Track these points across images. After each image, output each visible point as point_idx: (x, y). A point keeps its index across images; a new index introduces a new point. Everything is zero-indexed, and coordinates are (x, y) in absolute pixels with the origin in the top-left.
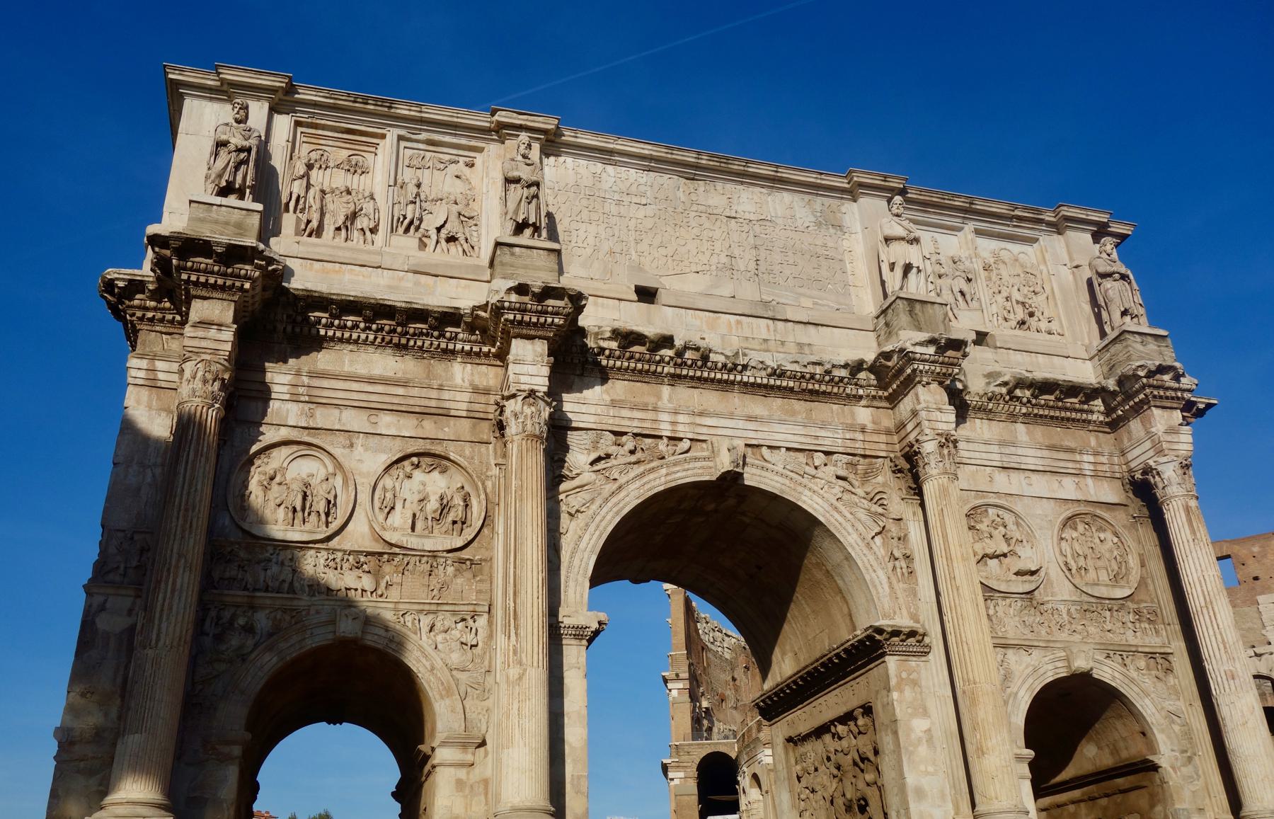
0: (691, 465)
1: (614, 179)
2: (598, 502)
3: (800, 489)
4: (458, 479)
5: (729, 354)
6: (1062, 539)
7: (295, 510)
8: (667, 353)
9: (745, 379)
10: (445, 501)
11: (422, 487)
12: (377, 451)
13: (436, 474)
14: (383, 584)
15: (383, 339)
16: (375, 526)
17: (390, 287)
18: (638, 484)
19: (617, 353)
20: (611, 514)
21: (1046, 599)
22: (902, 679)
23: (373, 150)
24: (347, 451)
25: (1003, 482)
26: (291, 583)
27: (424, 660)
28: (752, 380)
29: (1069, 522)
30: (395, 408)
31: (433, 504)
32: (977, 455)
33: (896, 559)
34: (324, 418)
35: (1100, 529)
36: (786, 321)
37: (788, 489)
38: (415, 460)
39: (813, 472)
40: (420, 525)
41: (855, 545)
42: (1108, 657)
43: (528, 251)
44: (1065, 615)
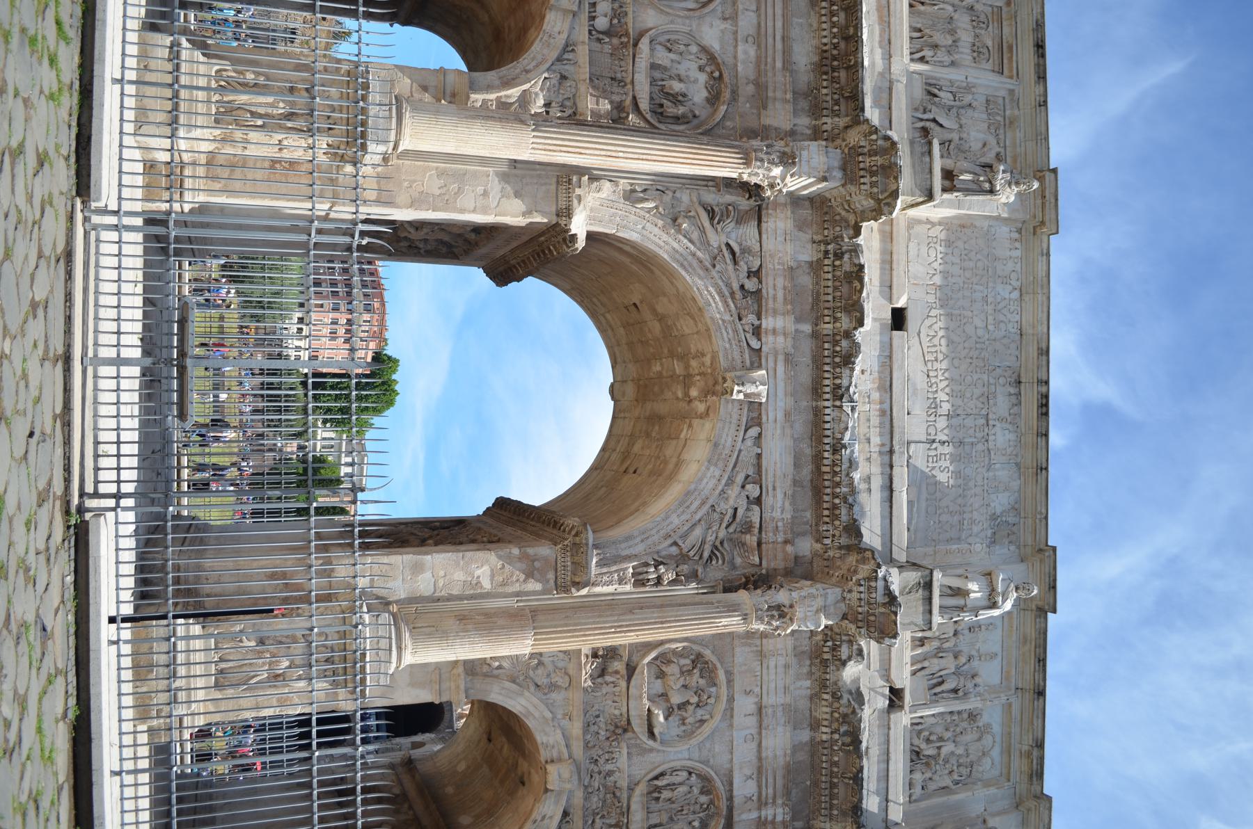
1: (1007, 296)
3: (721, 464)
5: (852, 390)
6: (690, 773)
9: (827, 411)
10: (680, 98)
11: (692, 79)
13: (705, 94)
15: (826, 51)
19: (838, 273)
20: (681, 259)
22: (533, 561)
23: (996, 69)
24: (719, 14)
25: (745, 705)
27: (534, 64)
31: (677, 86)
32: (772, 677)
37: (719, 451)
38: (717, 74)
40: (657, 75)
43: (927, 170)
44: (609, 767)
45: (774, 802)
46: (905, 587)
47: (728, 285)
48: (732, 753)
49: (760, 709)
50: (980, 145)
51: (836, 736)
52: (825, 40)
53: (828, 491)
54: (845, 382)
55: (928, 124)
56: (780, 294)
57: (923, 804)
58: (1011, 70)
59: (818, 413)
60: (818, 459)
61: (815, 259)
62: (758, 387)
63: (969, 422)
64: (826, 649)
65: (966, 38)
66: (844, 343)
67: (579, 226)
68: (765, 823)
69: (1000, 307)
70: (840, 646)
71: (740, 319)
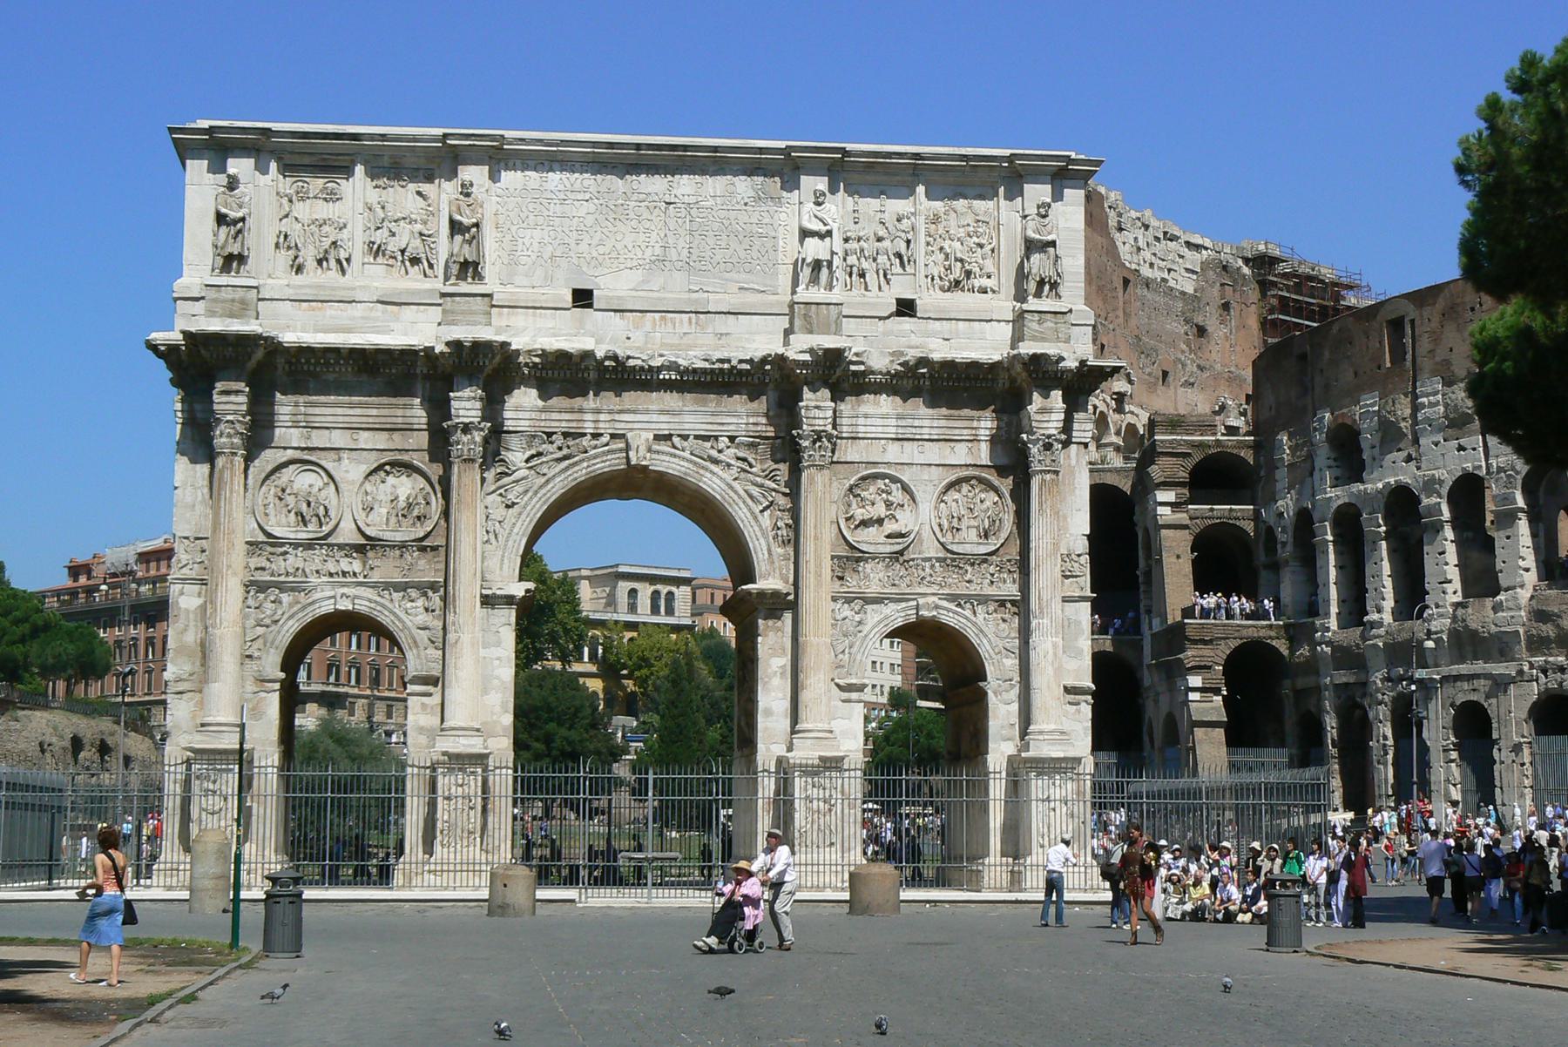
0: (609, 457)
2: (530, 494)
3: (702, 472)
4: (422, 482)
5: (645, 358)
6: (942, 501)
7: (303, 517)
12: (360, 462)
13: (404, 477)
14: (368, 567)
16: (359, 524)
17: (362, 318)
18: (563, 476)
19: (548, 367)
21: (912, 556)
25: (894, 453)
26: (303, 570)
28: (667, 377)
29: (953, 485)
30: (371, 426)
31: (402, 504)
32: (873, 429)
33: (778, 529)
34: (318, 439)
36: (709, 312)
38: (387, 468)
39: (714, 453)
42: (959, 605)
45: (976, 428)
47: (559, 460)
48: (930, 465)
50: (418, 198)
51: (927, 375)
52: (350, 369)
54: (639, 362)
57: (1003, 280)
58: (345, 160)
61: (535, 382)
62: (640, 439)
63: (672, 224)
64: (856, 381)
65: (323, 210)
66: (607, 363)
67: (519, 589)
69: (568, 185)
71: (586, 452)
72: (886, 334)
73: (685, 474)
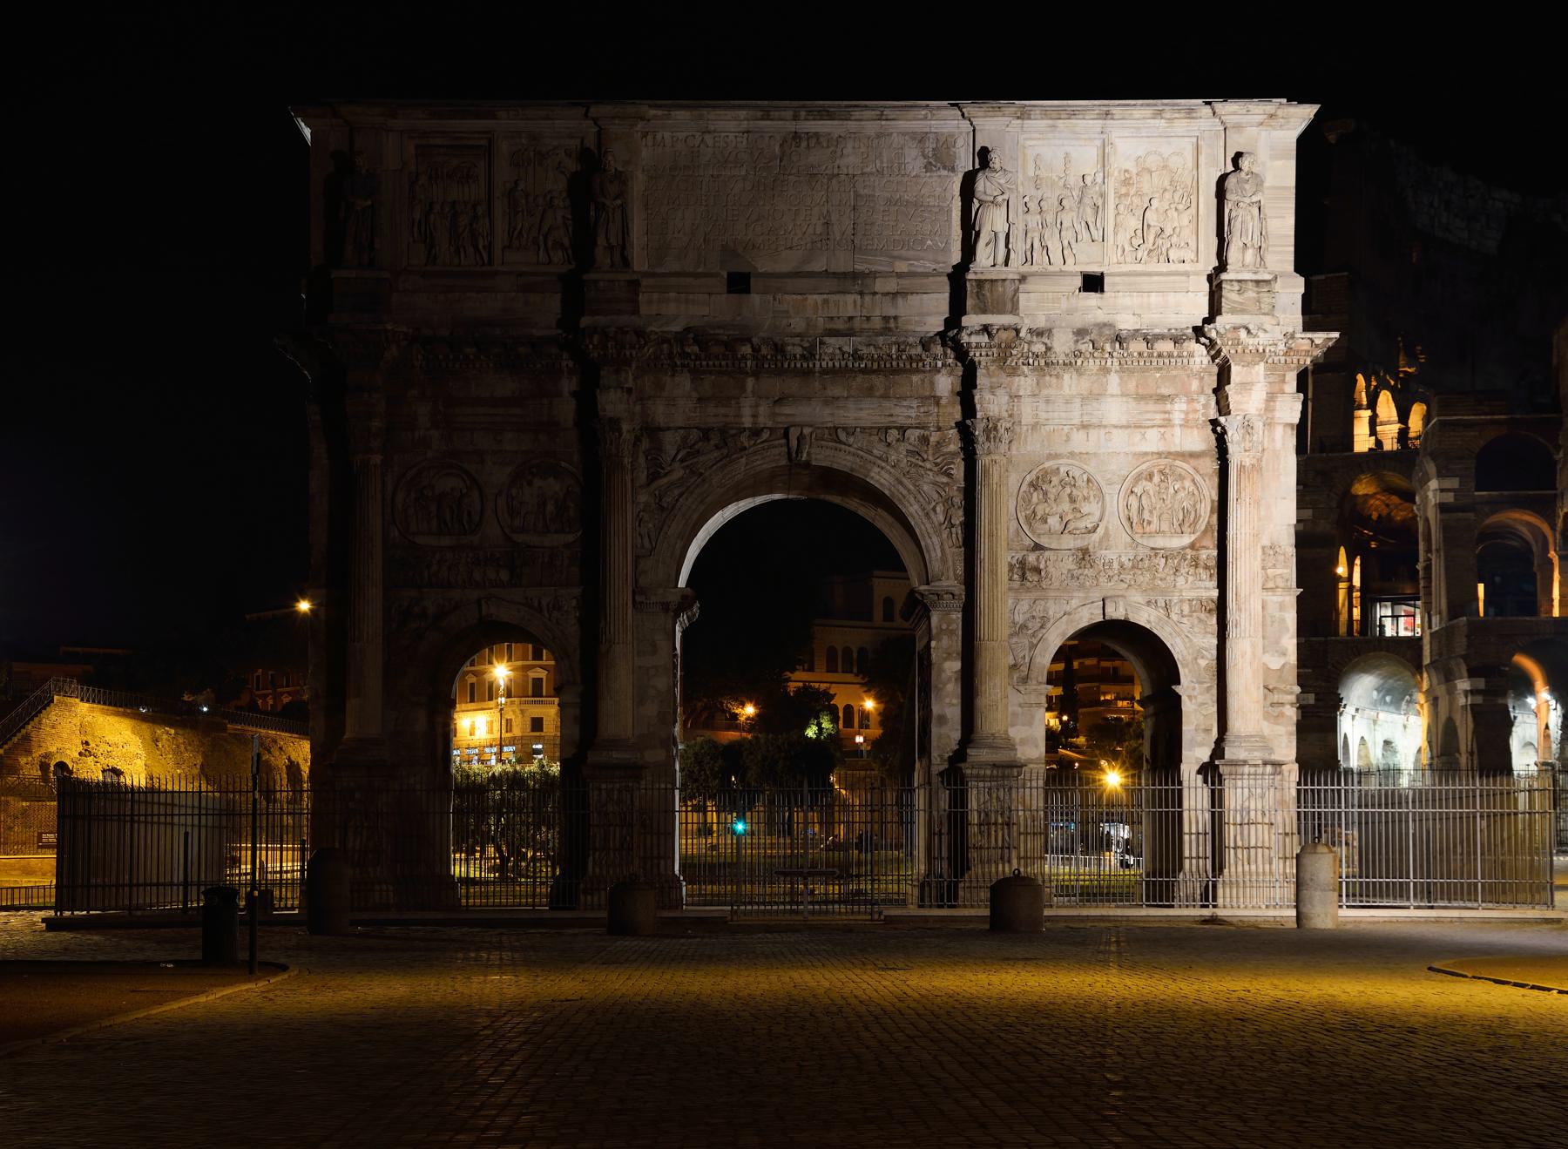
8: (746, 350)
13: (551, 480)
19: (703, 356)
31: (550, 507)
35: (1181, 478)
36: (875, 293)
41: (916, 515)
44: (1116, 565)
46: (980, 308)
49: (1084, 426)
51: (1115, 354)
53: (894, 363)
55: (550, 243)
56: (722, 411)
59: (824, 372)
60: (865, 371)
61: (688, 375)
68: (1187, 421)
70: (1033, 353)
71: (745, 449)
72: (1070, 312)
73: (852, 470)
